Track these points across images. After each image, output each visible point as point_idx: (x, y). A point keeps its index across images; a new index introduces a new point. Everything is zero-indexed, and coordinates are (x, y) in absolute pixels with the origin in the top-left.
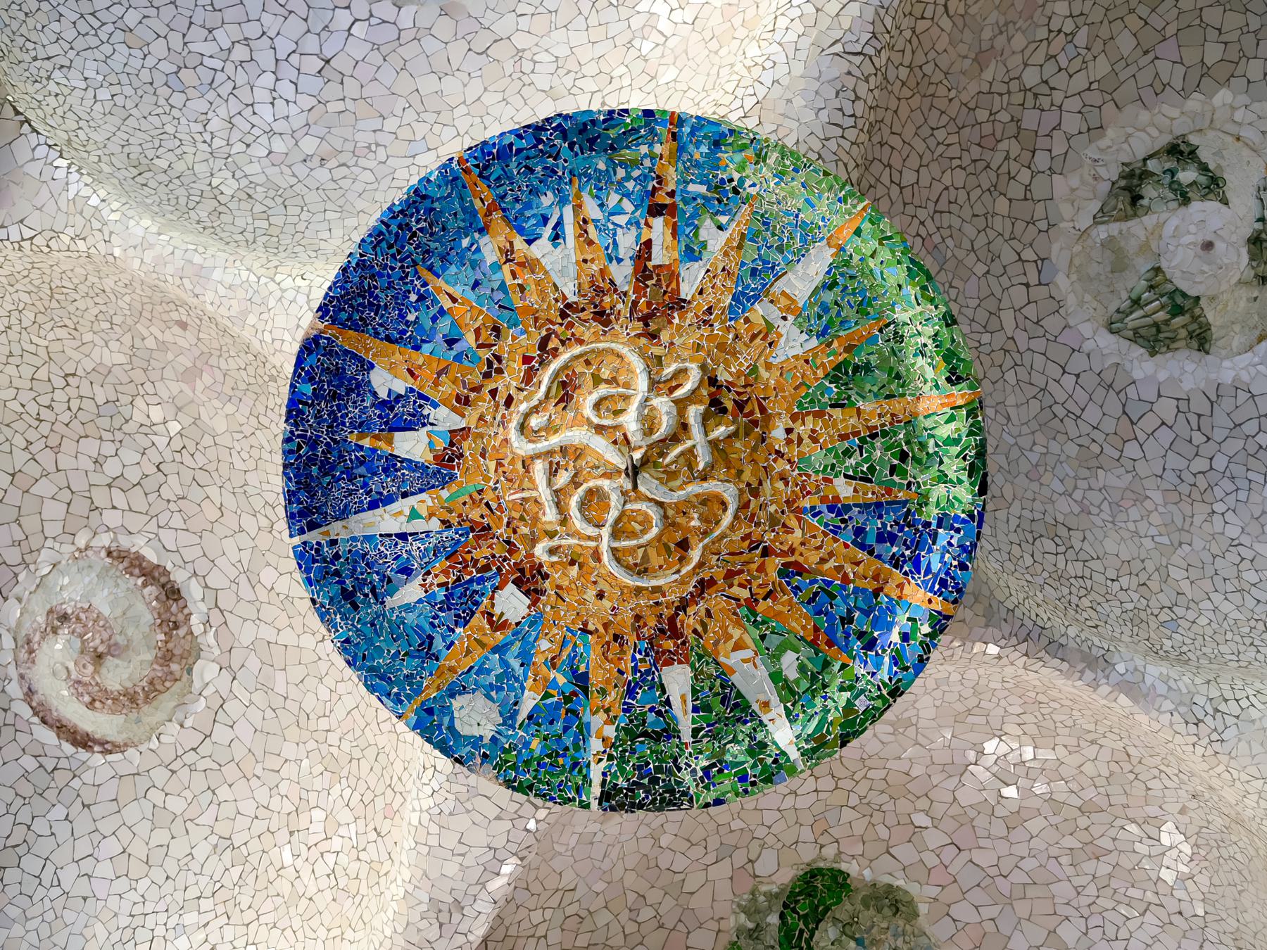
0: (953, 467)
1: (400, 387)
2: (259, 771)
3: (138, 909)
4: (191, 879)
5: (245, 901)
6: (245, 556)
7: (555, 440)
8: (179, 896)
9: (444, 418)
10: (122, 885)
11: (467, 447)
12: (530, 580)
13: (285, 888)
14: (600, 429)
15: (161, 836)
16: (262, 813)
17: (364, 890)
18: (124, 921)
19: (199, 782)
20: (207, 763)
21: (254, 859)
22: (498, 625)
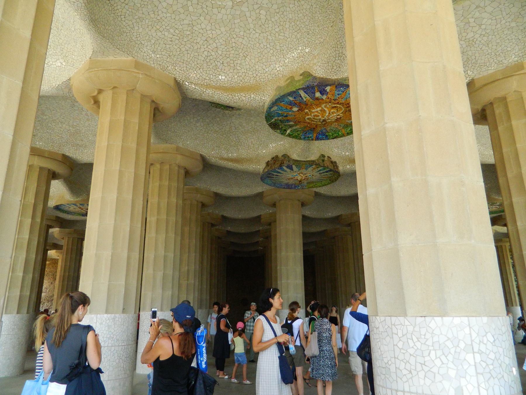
0: (335, 135)
1: (328, 91)
2: (213, 24)
3: (163, 18)
4: (179, 24)
5: (185, 40)
6: (266, 6)
7: (326, 109)
8: (173, 24)
9: (324, 97)
10: (165, 10)
11: (320, 101)
12: (301, 110)
13: (196, 48)
14: (329, 113)
15: (182, 11)
16: (205, 30)
17: (211, 67)
18: (159, 18)
19: (200, 11)
20: (206, 11)
21: (194, 35)
22: (291, 108)
